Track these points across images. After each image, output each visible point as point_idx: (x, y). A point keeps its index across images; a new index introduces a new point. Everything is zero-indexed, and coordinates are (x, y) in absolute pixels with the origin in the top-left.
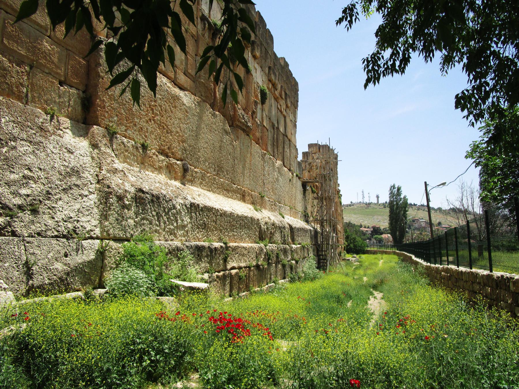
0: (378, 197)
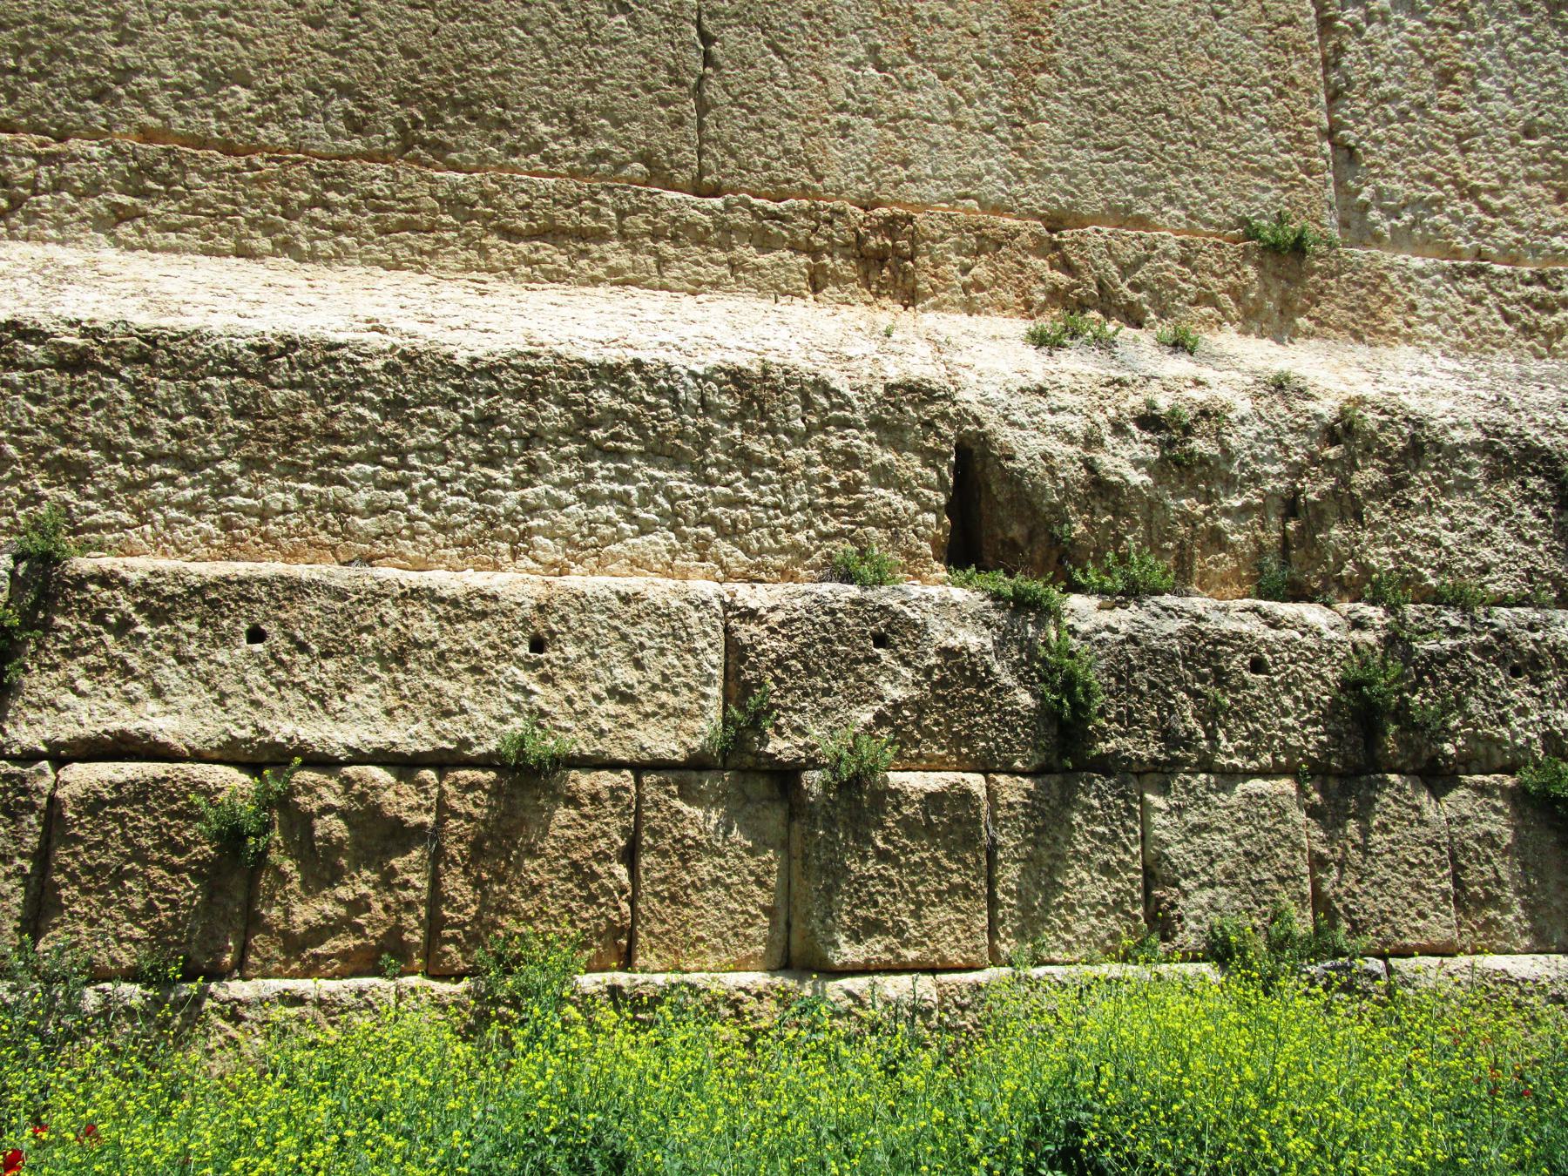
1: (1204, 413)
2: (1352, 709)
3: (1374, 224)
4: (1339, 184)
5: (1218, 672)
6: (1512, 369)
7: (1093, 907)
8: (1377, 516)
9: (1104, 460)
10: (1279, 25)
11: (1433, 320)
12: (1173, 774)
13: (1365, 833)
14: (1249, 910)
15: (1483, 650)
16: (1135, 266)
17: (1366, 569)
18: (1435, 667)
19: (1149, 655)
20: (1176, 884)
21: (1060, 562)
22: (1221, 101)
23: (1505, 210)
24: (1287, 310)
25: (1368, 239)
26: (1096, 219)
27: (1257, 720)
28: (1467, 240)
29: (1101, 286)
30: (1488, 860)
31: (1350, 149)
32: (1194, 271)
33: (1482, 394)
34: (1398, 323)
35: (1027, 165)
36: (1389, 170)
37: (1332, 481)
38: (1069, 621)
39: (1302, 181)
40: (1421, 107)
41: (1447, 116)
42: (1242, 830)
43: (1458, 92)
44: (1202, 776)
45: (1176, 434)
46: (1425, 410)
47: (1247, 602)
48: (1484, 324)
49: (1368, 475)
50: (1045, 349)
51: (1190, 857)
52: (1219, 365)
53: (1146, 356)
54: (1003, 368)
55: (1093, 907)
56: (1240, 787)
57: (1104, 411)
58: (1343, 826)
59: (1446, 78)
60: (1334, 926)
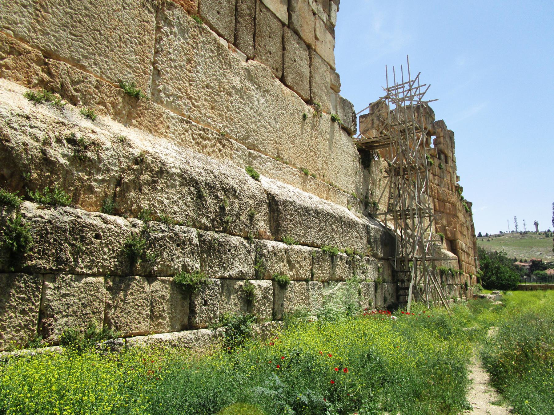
0: (536, 224)
1: (94, 143)
2: (127, 254)
3: (161, 97)
4: (154, 81)
5: (82, 237)
6: (192, 154)
7: (14, 327)
8: (146, 191)
9: (51, 151)
10: (144, 21)
11: (173, 133)
12: (58, 274)
13: (125, 296)
14: (80, 325)
15: (170, 238)
16: (78, 82)
17: (140, 208)
18: (155, 242)
19: (56, 229)
20: (52, 316)
21: (24, 187)
22: (120, 37)
23: (198, 107)
24: (130, 116)
25: (159, 101)
26: (64, 59)
27: (94, 256)
28: (187, 112)
29: (62, 85)
30: (162, 304)
31: (159, 71)
32: (100, 92)
33: (183, 159)
34: (164, 131)
35: (39, 28)
36: (168, 82)
37: (134, 176)
38: (23, 212)
39: (142, 75)
40: (181, 67)
41: (188, 73)
42: (82, 295)
43: (191, 67)
44: (70, 276)
45: (82, 148)
46: (166, 160)
47: (98, 213)
48: (187, 138)
49: (145, 177)
50: (33, 102)
51: (60, 306)
52: (102, 128)
53: (75, 117)
54: (11, 103)
55: (14, 327)
56: (84, 279)
57: (54, 132)
58: (118, 293)
59: (189, 61)
60: (110, 328)
